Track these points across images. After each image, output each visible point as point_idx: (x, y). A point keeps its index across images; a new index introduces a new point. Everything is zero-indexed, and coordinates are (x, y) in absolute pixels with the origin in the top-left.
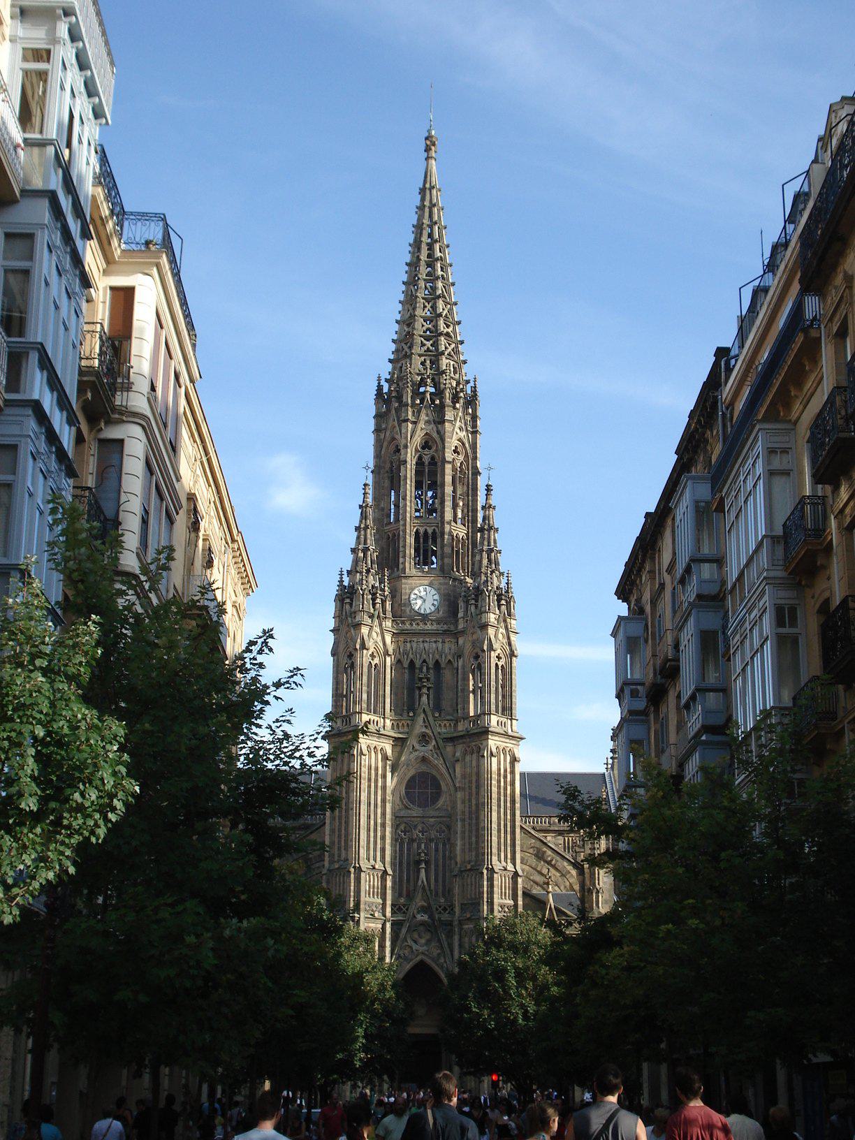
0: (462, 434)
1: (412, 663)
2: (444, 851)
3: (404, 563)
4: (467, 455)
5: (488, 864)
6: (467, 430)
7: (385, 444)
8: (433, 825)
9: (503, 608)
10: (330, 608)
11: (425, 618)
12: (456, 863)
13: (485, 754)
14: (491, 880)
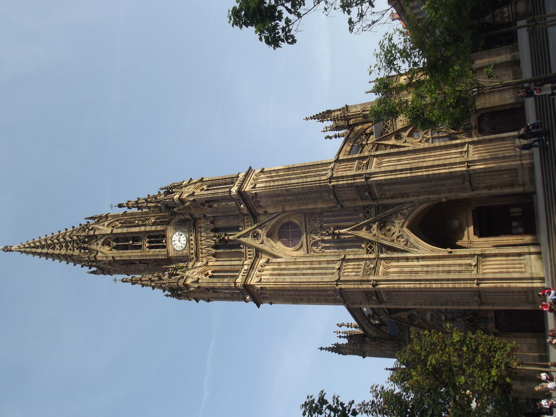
0: (106, 223)
1: (215, 247)
2: (328, 216)
3: (162, 256)
4: (117, 220)
5: (327, 182)
6: (105, 221)
7: (114, 268)
8: (312, 226)
9: (174, 190)
10: (184, 303)
11: (188, 240)
12: (334, 207)
13: (254, 192)
14: (338, 178)
